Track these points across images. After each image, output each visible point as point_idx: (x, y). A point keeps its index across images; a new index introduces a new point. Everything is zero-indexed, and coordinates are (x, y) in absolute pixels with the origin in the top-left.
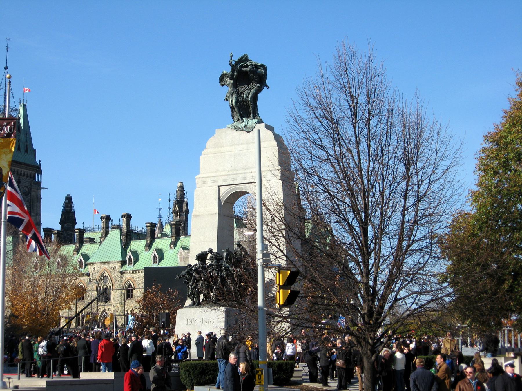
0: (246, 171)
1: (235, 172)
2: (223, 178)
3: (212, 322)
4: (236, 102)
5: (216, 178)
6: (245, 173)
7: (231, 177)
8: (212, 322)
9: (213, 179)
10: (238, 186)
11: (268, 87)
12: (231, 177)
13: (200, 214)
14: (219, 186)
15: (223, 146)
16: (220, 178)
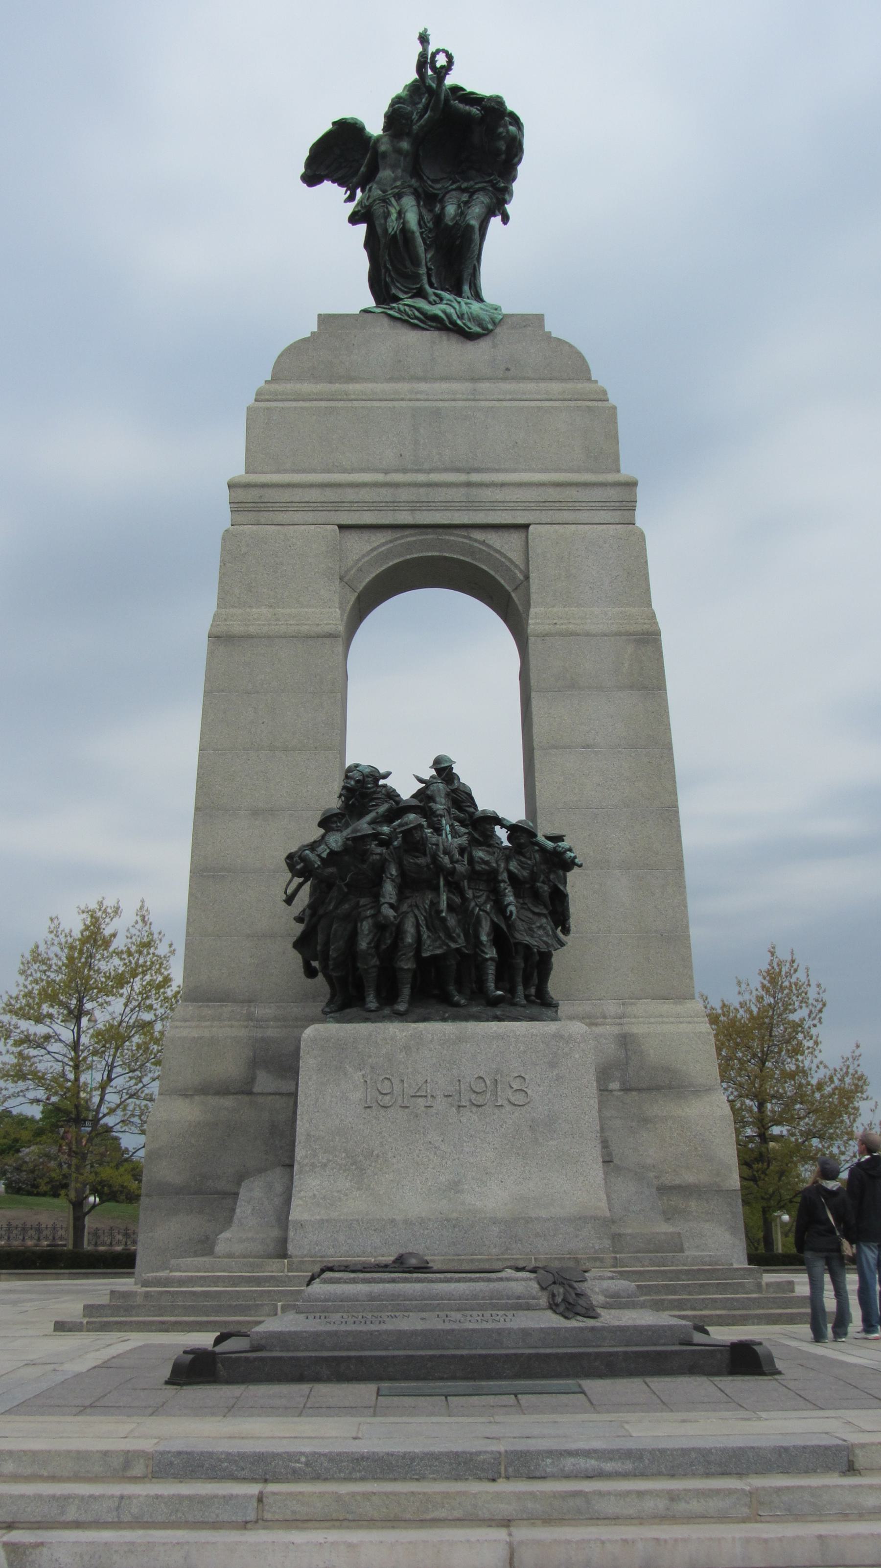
0: (475, 477)
1: (421, 478)
2: (365, 495)
3: (519, 1098)
4: (421, 222)
5: (330, 495)
6: (469, 484)
7: (405, 495)
8: (519, 1098)
9: (313, 495)
10: (430, 536)
11: (506, 219)
12: (405, 495)
13: (252, 630)
14: (341, 527)
15: (350, 379)
16: (350, 495)
